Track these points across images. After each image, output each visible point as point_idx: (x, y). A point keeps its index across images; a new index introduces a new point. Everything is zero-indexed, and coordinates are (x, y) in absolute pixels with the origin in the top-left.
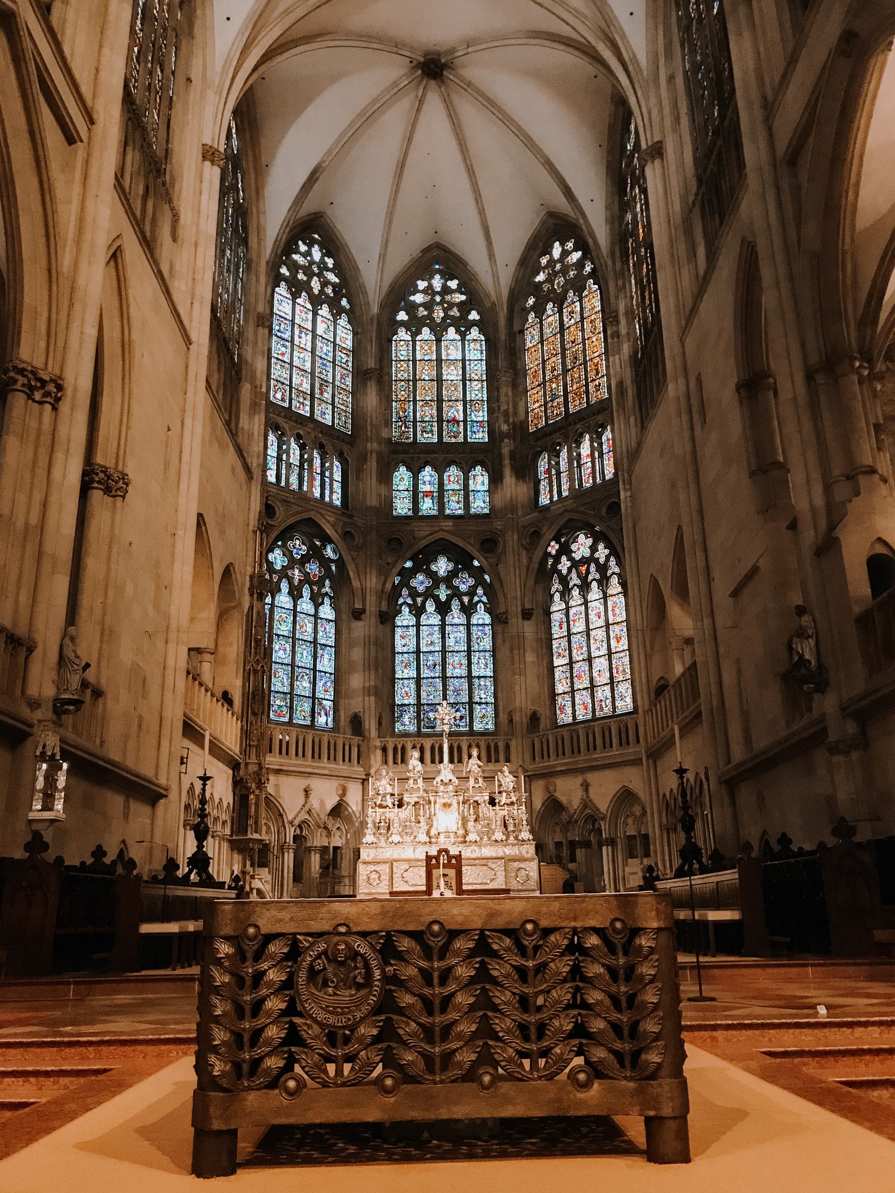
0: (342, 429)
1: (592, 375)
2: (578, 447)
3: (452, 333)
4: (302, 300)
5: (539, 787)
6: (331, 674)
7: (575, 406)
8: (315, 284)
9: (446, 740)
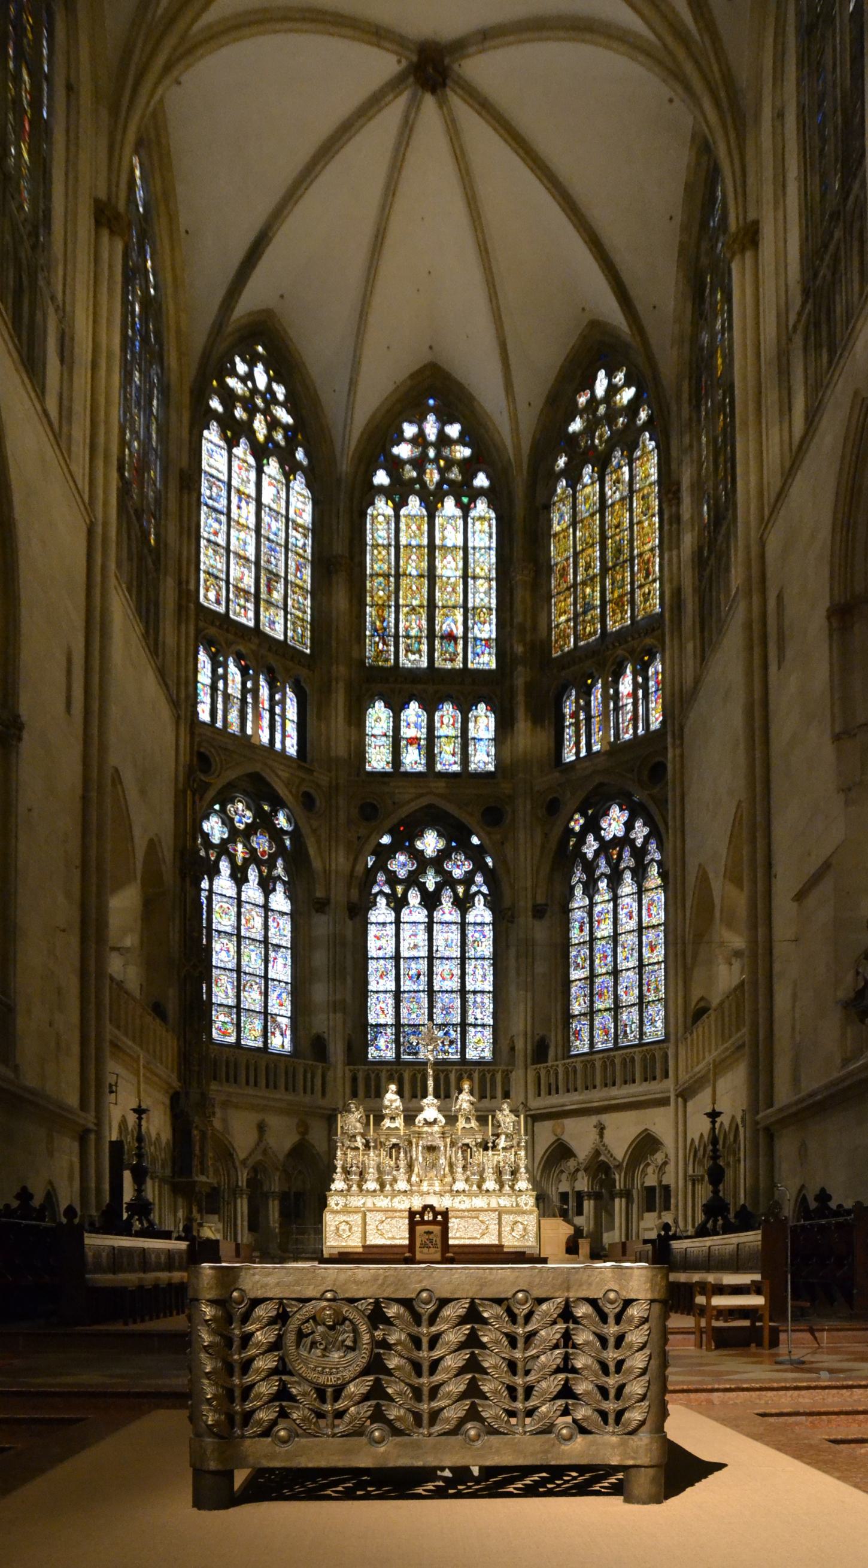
0: (299, 647)
1: (640, 577)
2: (616, 683)
3: (449, 503)
4: (241, 450)
5: (546, 1134)
6: (286, 983)
7: (615, 622)
8: (260, 426)
9: (430, 1072)
